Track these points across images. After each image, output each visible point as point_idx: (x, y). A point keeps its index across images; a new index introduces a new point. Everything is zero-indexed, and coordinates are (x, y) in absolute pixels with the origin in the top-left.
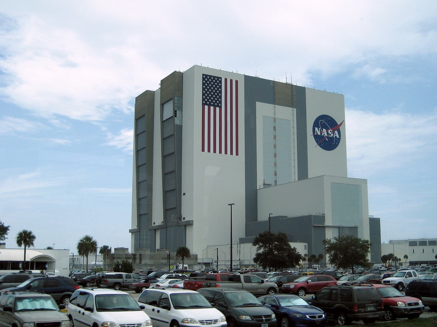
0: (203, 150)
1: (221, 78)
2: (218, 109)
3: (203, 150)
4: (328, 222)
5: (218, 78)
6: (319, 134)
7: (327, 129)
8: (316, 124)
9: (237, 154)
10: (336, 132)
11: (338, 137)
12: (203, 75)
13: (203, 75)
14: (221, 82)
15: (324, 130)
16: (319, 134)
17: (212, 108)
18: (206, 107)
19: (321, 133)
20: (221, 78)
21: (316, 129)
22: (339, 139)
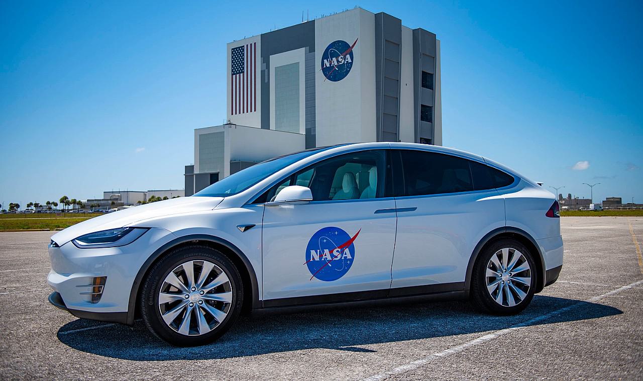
0: (232, 114)
1: (244, 46)
2: (242, 74)
3: (232, 114)
4: (197, 171)
5: (242, 47)
6: (328, 65)
7: (337, 57)
8: (325, 56)
9: (255, 111)
10: (348, 56)
11: (350, 61)
12: (232, 49)
13: (232, 49)
14: (243, 50)
15: (334, 59)
16: (328, 65)
17: (238, 75)
18: (234, 76)
19: (330, 65)
20: (244, 46)
21: (325, 61)
22: (351, 63)
